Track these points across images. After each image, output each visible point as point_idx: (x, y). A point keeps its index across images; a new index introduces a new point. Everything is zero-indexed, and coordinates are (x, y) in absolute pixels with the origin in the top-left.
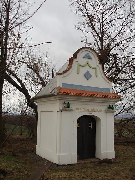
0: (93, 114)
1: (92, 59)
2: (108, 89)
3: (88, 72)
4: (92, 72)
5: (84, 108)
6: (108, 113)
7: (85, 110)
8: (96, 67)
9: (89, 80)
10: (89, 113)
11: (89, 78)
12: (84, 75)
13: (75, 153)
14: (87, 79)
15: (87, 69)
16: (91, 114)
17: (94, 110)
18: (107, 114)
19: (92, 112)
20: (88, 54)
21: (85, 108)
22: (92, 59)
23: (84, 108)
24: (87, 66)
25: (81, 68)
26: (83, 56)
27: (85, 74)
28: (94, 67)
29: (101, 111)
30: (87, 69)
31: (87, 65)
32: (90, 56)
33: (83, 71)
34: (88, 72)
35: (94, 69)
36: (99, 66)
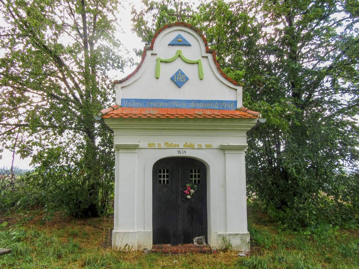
0: (190, 153)
1: (190, 45)
2: (231, 102)
3: (179, 73)
4: (190, 71)
5: (166, 144)
6: (226, 152)
7: (169, 147)
8: (200, 60)
9: (182, 88)
10: (179, 152)
11: (183, 83)
12: (172, 79)
13: (150, 229)
14: (177, 85)
15: (178, 65)
16: (184, 155)
17: (192, 147)
18: (225, 154)
19: (186, 150)
20: (179, 36)
21: (170, 143)
22: (190, 45)
23: (166, 144)
24: (179, 61)
25: (163, 66)
26: (169, 43)
27: (173, 76)
28: (195, 60)
29: (209, 147)
30: (178, 65)
31: (179, 59)
32: (185, 40)
33: (168, 71)
34: (179, 73)
35: (196, 66)
36: (207, 57)
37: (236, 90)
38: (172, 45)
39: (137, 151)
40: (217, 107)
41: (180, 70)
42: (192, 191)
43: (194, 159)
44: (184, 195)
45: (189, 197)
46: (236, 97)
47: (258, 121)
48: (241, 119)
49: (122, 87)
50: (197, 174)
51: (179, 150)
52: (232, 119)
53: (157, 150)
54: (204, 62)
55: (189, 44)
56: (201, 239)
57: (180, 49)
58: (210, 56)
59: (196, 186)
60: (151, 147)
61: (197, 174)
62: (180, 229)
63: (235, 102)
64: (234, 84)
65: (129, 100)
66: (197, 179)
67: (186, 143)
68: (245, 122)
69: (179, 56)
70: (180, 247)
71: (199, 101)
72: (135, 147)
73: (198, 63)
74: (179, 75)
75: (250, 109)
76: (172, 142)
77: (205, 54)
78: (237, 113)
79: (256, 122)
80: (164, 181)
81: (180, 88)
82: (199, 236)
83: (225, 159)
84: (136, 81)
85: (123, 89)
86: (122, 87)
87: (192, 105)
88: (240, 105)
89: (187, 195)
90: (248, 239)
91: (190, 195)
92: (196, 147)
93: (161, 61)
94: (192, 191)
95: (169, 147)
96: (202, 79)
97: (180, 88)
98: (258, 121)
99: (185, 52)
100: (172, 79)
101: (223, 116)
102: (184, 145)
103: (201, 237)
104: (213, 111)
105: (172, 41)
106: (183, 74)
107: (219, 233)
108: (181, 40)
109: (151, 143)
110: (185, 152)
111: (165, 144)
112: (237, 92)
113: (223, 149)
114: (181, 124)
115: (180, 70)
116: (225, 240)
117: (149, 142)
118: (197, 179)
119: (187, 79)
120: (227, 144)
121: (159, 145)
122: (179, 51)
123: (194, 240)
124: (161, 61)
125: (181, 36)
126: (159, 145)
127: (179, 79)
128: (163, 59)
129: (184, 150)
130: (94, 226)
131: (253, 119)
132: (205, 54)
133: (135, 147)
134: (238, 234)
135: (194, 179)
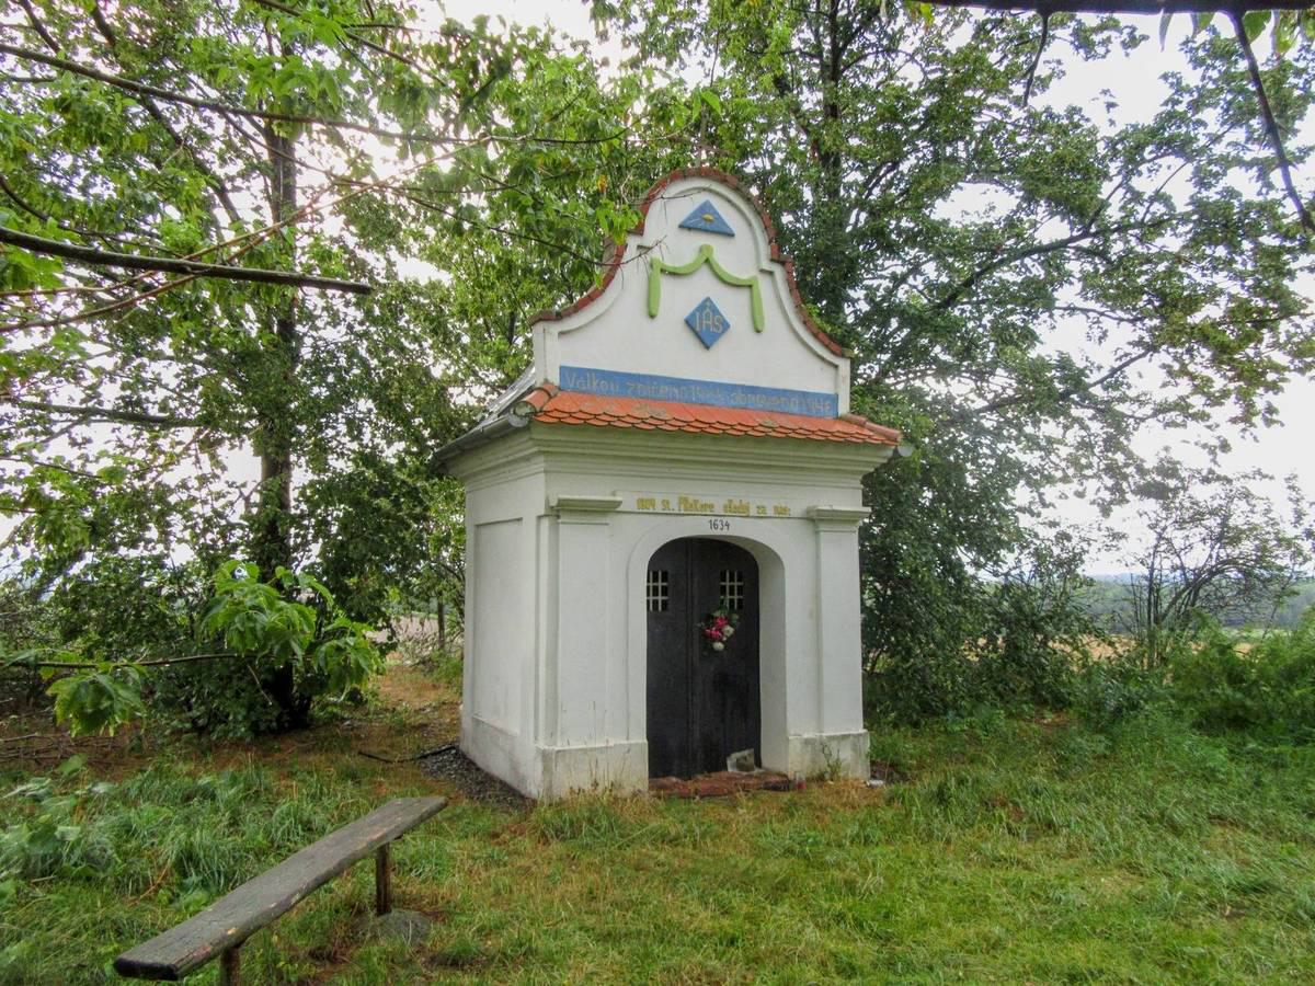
0: (738, 529)
1: (731, 235)
2: (826, 397)
3: (707, 306)
4: (732, 306)
5: (683, 500)
6: (822, 527)
7: (690, 509)
8: (755, 278)
9: (714, 348)
10: (715, 526)
11: (716, 337)
12: (689, 323)
13: (640, 739)
14: (702, 341)
15: (702, 287)
16: (725, 532)
17: (742, 512)
18: (817, 533)
19: (729, 520)
20: (705, 208)
21: (691, 500)
22: (731, 235)
23: (683, 500)
24: (704, 275)
25: (666, 285)
26: (681, 219)
27: (693, 315)
28: (744, 277)
29: (782, 513)
30: (702, 287)
31: (705, 270)
32: (719, 218)
33: (679, 300)
34: (707, 306)
35: (744, 295)
36: (771, 273)
37: (836, 367)
38: (690, 229)
39: (607, 519)
40: (795, 409)
41: (708, 299)
42: (729, 630)
43: (738, 548)
44: (707, 640)
45: (719, 646)
46: (836, 386)
47: (896, 451)
48: (844, 443)
49: (562, 334)
50: (736, 584)
51: (713, 519)
52: (828, 442)
53: (659, 517)
54: (763, 285)
55: (725, 230)
56: (745, 758)
57: (708, 243)
58: (778, 271)
59: (736, 617)
60: (645, 508)
61: (736, 584)
62: (697, 735)
63: (834, 399)
64: (833, 353)
65: (581, 372)
66: (736, 597)
67: (730, 501)
68: (866, 451)
69: (707, 261)
70: (702, 782)
71: (754, 390)
72: (607, 509)
73: (750, 286)
74: (708, 313)
75: (872, 420)
76: (697, 498)
77: (767, 265)
78: (838, 427)
79: (889, 453)
80: (732, 601)
81: (707, 347)
82: (740, 750)
83: (817, 544)
84: (597, 318)
85: (565, 338)
86: (562, 334)
87: (739, 400)
88: (844, 407)
89: (714, 640)
90: (866, 746)
91: (721, 641)
92: (753, 512)
93: (662, 271)
94: (729, 630)
95: (690, 509)
96: (654, 312)
97: (707, 347)
98: (896, 451)
99: (719, 249)
100: (689, 323)
101: (635, 421)
102: (725, 507)
103: (746, 753)
104: (776, 416)
105: (689, 218)
106: (715, 311)
107: (806, 736)
108: (711, 217)
109: (645, 497)
110: (728, 525)
111: (680, 503)
112: (837, 374)
113: (816, 520)
114: (744, 450)
115: (708, 299)
116: (826, 751)
117: (641, 496)
118: (736, 597)
119: (726, 326)
120: (828, 508)
121: (666, 503)
122: (708, 248)
123: (729, 762)
124: (662, 271)
125: (711, 207)
126: (666, 503)
127: (708, 326)
128: (669, 264)
129: (724, 520)
130: (360, 753)
131: (884, 446)
132: (767, 265)
133: (607, 509)
134: (848, 736)
135: (728, 597)
